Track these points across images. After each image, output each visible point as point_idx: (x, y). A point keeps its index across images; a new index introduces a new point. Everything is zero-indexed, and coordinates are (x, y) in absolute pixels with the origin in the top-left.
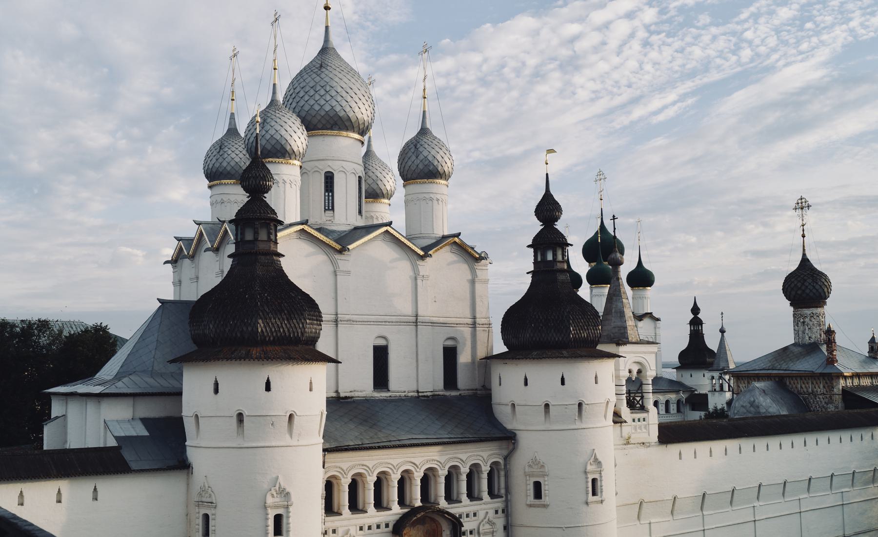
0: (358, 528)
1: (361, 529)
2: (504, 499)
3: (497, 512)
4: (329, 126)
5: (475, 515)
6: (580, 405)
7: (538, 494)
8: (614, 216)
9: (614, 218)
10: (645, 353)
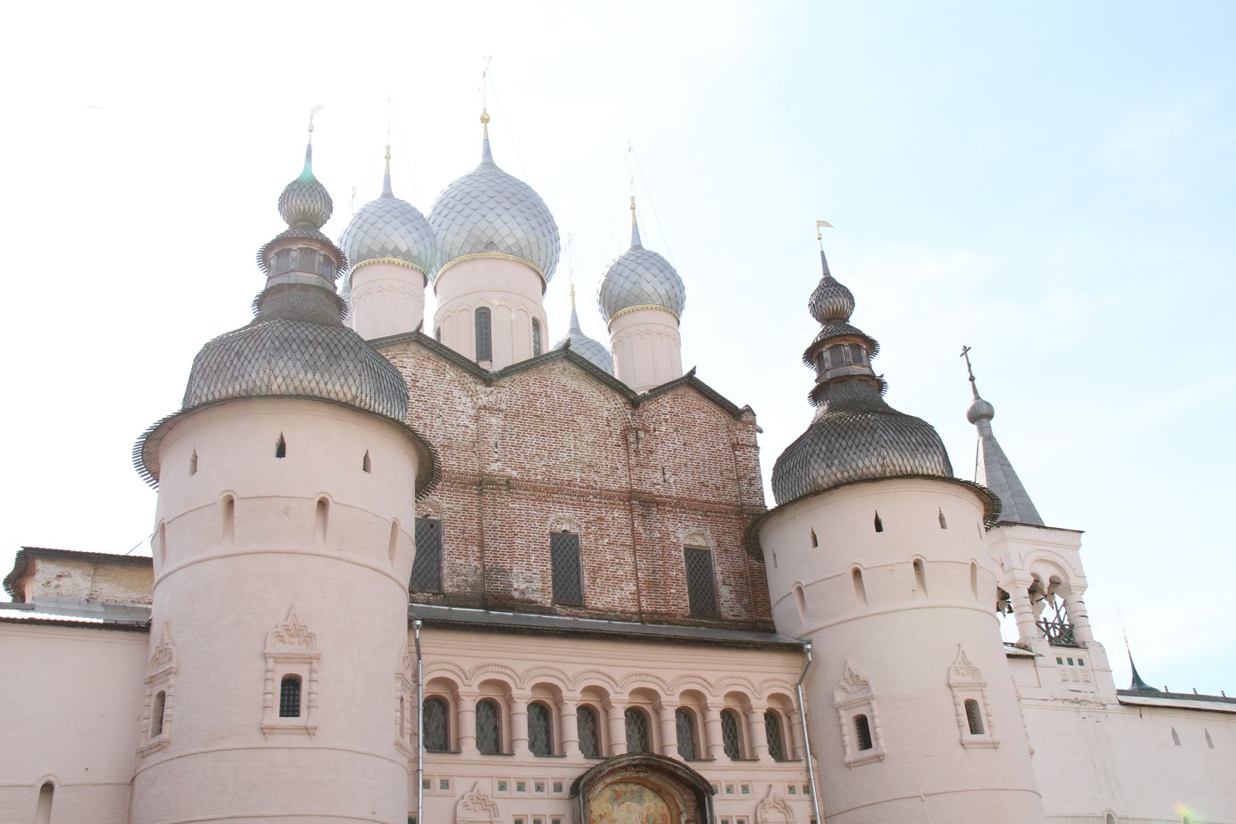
0: (497, 786)
1: (502, 787)
2: (803, 764)
3: (792, 789)
4: (481, 247)
5: (745, 789)
6: (917, 564)
7: (865, 741)
8: (965, 347)
9: (966, 350)
10: (1058, 545)
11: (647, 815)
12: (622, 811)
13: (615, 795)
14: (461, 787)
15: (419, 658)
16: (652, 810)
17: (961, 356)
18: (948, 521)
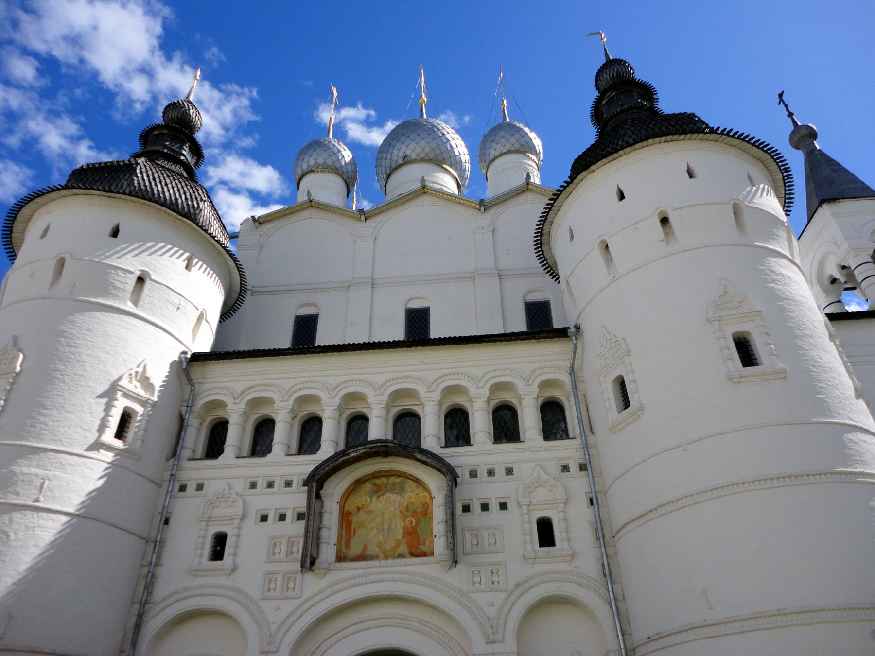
1: (253, 486)
3: (565, 468)
5: (509, 471)
11: (408, 504)
12: (381, 502)
13: (376, 488)
14: (211, 488)
15: (192, 385)
16: (413, 500)
17: (779, 104)
18: (697, 171)
